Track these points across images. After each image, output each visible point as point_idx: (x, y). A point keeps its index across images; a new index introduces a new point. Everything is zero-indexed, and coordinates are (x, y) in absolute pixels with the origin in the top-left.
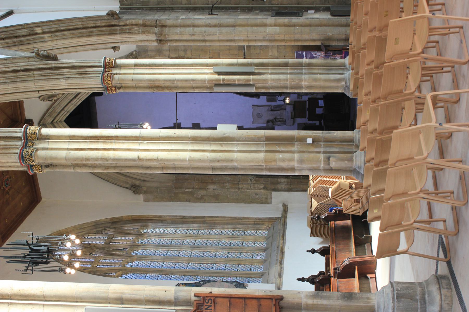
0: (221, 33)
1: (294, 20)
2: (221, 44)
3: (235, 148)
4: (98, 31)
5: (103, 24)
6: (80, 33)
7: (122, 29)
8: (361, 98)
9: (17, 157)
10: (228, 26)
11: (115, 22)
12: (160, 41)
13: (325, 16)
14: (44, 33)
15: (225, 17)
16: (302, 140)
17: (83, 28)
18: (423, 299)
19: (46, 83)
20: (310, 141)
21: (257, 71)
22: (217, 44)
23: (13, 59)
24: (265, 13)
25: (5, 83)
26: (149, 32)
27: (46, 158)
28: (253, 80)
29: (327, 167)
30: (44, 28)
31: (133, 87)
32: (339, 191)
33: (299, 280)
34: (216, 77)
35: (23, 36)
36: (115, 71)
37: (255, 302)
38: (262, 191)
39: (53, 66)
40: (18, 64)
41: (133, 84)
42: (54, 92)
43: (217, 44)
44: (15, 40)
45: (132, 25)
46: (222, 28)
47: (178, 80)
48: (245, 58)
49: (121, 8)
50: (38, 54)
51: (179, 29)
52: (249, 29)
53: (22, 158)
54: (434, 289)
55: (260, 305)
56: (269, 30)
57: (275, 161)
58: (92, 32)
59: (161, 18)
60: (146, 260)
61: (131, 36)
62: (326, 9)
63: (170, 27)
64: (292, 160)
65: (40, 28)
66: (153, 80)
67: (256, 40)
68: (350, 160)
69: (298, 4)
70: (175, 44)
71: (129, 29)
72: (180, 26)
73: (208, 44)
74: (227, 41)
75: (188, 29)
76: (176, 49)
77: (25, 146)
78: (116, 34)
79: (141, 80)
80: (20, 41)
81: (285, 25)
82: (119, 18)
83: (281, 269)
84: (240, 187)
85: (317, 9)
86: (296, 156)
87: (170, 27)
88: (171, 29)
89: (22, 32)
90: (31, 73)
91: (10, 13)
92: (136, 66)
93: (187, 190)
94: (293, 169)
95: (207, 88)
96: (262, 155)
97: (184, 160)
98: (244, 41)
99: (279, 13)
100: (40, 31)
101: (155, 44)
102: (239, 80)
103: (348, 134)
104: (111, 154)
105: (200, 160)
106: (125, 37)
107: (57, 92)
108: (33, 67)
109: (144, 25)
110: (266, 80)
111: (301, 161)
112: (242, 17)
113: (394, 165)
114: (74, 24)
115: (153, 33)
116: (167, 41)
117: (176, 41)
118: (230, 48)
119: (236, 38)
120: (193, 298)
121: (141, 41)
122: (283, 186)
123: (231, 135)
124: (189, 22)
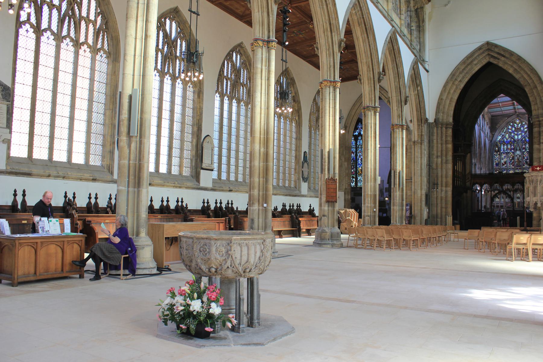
0: (418, 170)
1: (424, 203)
2: (413, 170)
3: (372, 184)
4: (419, 114)
5: (422, 117)
6: (418, 106)
7: (420, 125)
8: (390, 226)
9: (368, 105)
10: (421, 173)
11: (423, 121)
12: (414, 142)
13: (425, 216)
14: (418, 90)
15: (425, 172)
16: (375, 207)
17: (420, 107)
18: (338, 240)
19: (395, 101)
20: (375, 210)
21: (400, 188)
22: (413, 168)
23: (405, 87)
24: (427, 190)
25: (395, 85)
26: (418, 138)
27: (368, 115)
28: (397, 187)
29: (365, 216)
30: (420, 90)
31: (393, 136)
32: (350, 222)
33: (310, 205)
34: (398, 172)
35: (416, 82)
36: (400, 129)
37: (335, 195)
38: (344, 187)
39: (402, 104)
40: (403, 89)
41: (395, 136)
42: (391, 103)
43: (413, 168)
44: (414, 79)
45: (422, 130)
46: (420, 170)
47: (396, 156)
48: (406, 180)
49: (430, 123)
50: (407, 97)
51: (419, 151)
52: (420, 183)
53: (368, 107)
54: (340, 243)
55: (334, 197)
56: (419, 191)
57: (368, 198)
58: (419, 112)
59: (425, 143)
60: (314, 136)
61: (417, 129)
62: (429, 217)
63: (421, 147)
64: (368, 204)
65: (420, 89)
66: (396, 146)
67: (414, 185)
68: (368, 224)
69: (431, 205)
70: (413, 149)
71: (420, 128)
72: (421, 152)
73: (413, 164)
74: (414, 173)
75: (420, 155)
76: (411, 148)
77: (372, 107)
78: (418, 122)
79: (396, 141)
80: (414, 81)
81: (421, 199)
82: (425, 123)
83: (313, 197)
84: (346, 177)
85: (429, 213)
86: (370, 205)
87: (421, 147)
88: (420, 147)
89: (418, 82)
90: (399, 95)
91: (427, 71)
92: (403, 138)
93: (344, 152)
94: (364, 204)
95: (393, 167)
96: (370, 193)
97: (368, 165)
98: (414, 180)
99: (427, 196)
100: (418, 89)
101: (413, 140)
102: (396, 181)
103: (377, 223)
104: (370, 139)
105: (368, 171)
106: (416, 126)
107: (391, 105)
108: (402, 96)
109: (422, 135)
110: (396, 192)
111: (368, 207)
112: (425, 180)
113: (375, 230)
114: (422, 103)
115: (418, 139)
116: (414, 145)
117: (414, 150)
118: (411, 173)
119: (415, 177)
120: (336, 178)
121: (414, 134)
122: (347, 197)
123: (377, 182)
124: (423, 155)
